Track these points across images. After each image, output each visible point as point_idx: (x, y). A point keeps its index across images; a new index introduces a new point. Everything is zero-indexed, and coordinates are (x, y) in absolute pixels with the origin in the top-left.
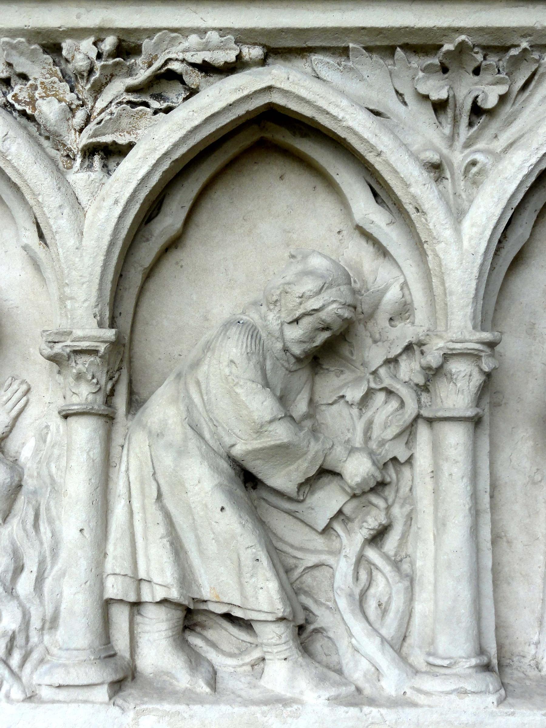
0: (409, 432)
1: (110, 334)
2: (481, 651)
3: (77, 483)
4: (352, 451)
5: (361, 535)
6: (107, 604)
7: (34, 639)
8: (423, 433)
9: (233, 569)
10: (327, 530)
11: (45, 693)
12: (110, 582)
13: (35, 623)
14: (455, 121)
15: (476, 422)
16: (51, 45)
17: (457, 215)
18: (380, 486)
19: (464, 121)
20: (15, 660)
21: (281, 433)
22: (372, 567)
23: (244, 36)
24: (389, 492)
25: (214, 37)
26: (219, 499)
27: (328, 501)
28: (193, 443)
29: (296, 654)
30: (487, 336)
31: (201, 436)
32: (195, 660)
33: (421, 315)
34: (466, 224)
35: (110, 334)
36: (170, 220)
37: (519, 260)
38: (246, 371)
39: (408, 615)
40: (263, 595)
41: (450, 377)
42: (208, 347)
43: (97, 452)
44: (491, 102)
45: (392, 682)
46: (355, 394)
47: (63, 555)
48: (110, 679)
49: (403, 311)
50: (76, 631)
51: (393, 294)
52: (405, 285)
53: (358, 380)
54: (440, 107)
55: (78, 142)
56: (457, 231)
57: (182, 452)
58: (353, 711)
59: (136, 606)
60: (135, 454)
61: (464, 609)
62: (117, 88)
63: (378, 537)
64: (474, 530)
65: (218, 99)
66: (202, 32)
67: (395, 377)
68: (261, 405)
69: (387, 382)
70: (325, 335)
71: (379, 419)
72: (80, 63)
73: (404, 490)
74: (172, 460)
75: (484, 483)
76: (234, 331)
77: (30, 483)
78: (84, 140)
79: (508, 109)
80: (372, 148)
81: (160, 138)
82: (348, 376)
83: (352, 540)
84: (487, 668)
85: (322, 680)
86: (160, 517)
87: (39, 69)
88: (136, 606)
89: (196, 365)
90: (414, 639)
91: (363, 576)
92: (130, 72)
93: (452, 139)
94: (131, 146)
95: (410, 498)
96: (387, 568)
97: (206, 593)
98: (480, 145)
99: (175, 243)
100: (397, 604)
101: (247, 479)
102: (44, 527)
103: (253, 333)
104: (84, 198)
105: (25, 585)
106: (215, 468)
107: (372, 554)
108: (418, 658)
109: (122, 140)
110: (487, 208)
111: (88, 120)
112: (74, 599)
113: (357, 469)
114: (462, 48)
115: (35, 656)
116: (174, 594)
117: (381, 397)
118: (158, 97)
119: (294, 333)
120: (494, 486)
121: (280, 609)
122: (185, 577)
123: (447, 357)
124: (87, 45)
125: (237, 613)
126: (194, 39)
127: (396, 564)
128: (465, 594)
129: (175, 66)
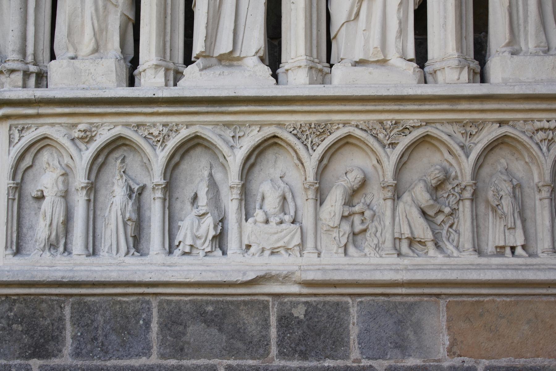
0: (458, 203)
1: (395, 182)
2: (474, 247)
3: (389, 213)
4: (446, 206)
5: (448, 225)
6: (395, 239)
7: (380, 245)
8: (461, 203)
9: (422, 230)
10: (440, 224)
11: (384, 256)
12: (395, 234)
13: (380, 242)
14: (466, 137)
15: (472, 200)
16: (381, 122)
17: (467, 156)
18: (451, 214)
19: (468, 137)
20: (377, 249)
21: (431, 202)
22: (450, 233)
23: (422, 121)
24: (454, 216)
25: (416, 121)
26: (419, 216)
27: (440, 218)
28: (413, 204)
29: (435, 248)
30: (474, 182)
31: (414, 202)
32: (413, 252)
33: (460, 178)
34: (469, 159)
35: (395, 182)
36: (405, 158)
37: (481, 166)
38: (424, 189)
39: (459, 241)
40: (429, 235)
41: (467, 191)
42: (416, 185)
43: (392, 207)
44: (474, 133)
45: (456, 253)
46: (446, 195)
47: (386, 228)
48: (397, 253)
49: (456, 177)
50: (389, 244)
51: (454, 174)
52: (456, 172)
53: (446, 193)
54: (462, 134)
55: (386, 142)
56: (468, 160)
57: (411, 206)
58: (448, 258)
59: (400, 239)
60: (401, 206)
61: (471, 239)
62: (395, 131)
63: (451, 226)
64: (472, 223)
65: (416, 134)
66: (413, 120)
67: (454, 191)
68: (427, 196)
69: (453, 192)
70: (440, 182)
71: (451, 200)
72: (388, 126)
73: (457, 216)
74: (408, 208)
75: (474, 214)
76: (421, 181)
77: (377, 214)
78: (389, 142)
79: (478, 134)
80: (449, 143)
81: (405, 142)
82: (444, 192)
83: (446, 227)
84: (476, 251)
85: (441, 253)
86: (406, 220)
87: (378, 127)
88: (400, 239)
89: (413, 188)
90: (460, 246)
91: (448, 234)
92: (398, 128)
93: (466, 140)
94: (398, 143)
95: (458, 217)
96: (454, 232)
97: (416, 236)
98: (472, 142)
99: (405, 163)
100: (456, 238)
101: (424, 213)
102: (382, 222)
103: (425, 181)
104: (389, 154)
105: (378, 234)
106: (418, 209)
107: (450, 230)
108: (461, 250)
109: (396, 142)
110: (473, 156)
111: (389, 138)
112: (388, 237)
113: (447, 210)
114: (467, 122)
115: (381, 249)
116: (410, 236)
117: (451, 195)
118: (403, 133)
119: (433, 182)
120: (476, 215)
121: (432, 238)
122: (412, 233)
123: (465, 187)
124: (389, 122)
125: (423, 241)
126: (411, 121)
127: (456, 231)
128: (471, 235)
129: (408, 127)
